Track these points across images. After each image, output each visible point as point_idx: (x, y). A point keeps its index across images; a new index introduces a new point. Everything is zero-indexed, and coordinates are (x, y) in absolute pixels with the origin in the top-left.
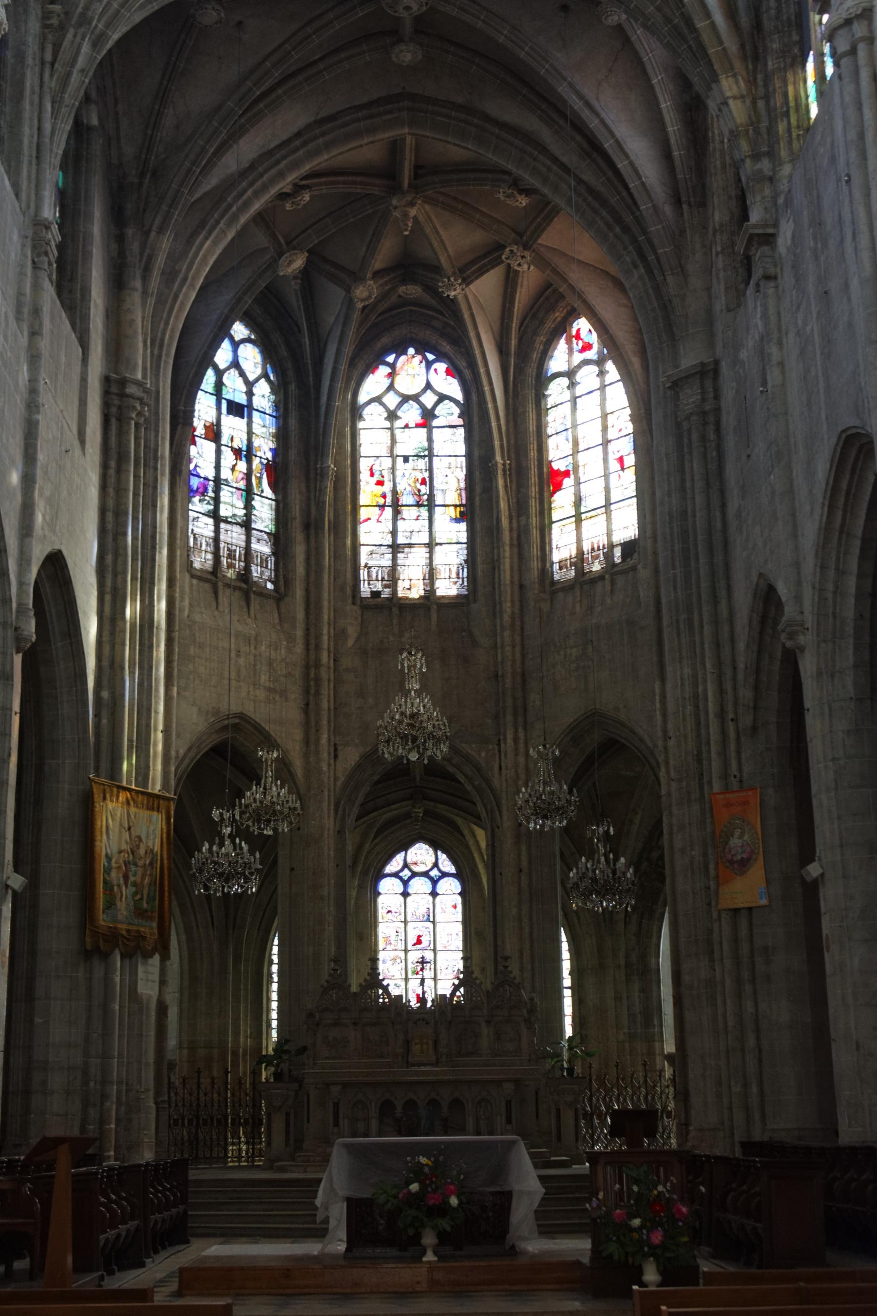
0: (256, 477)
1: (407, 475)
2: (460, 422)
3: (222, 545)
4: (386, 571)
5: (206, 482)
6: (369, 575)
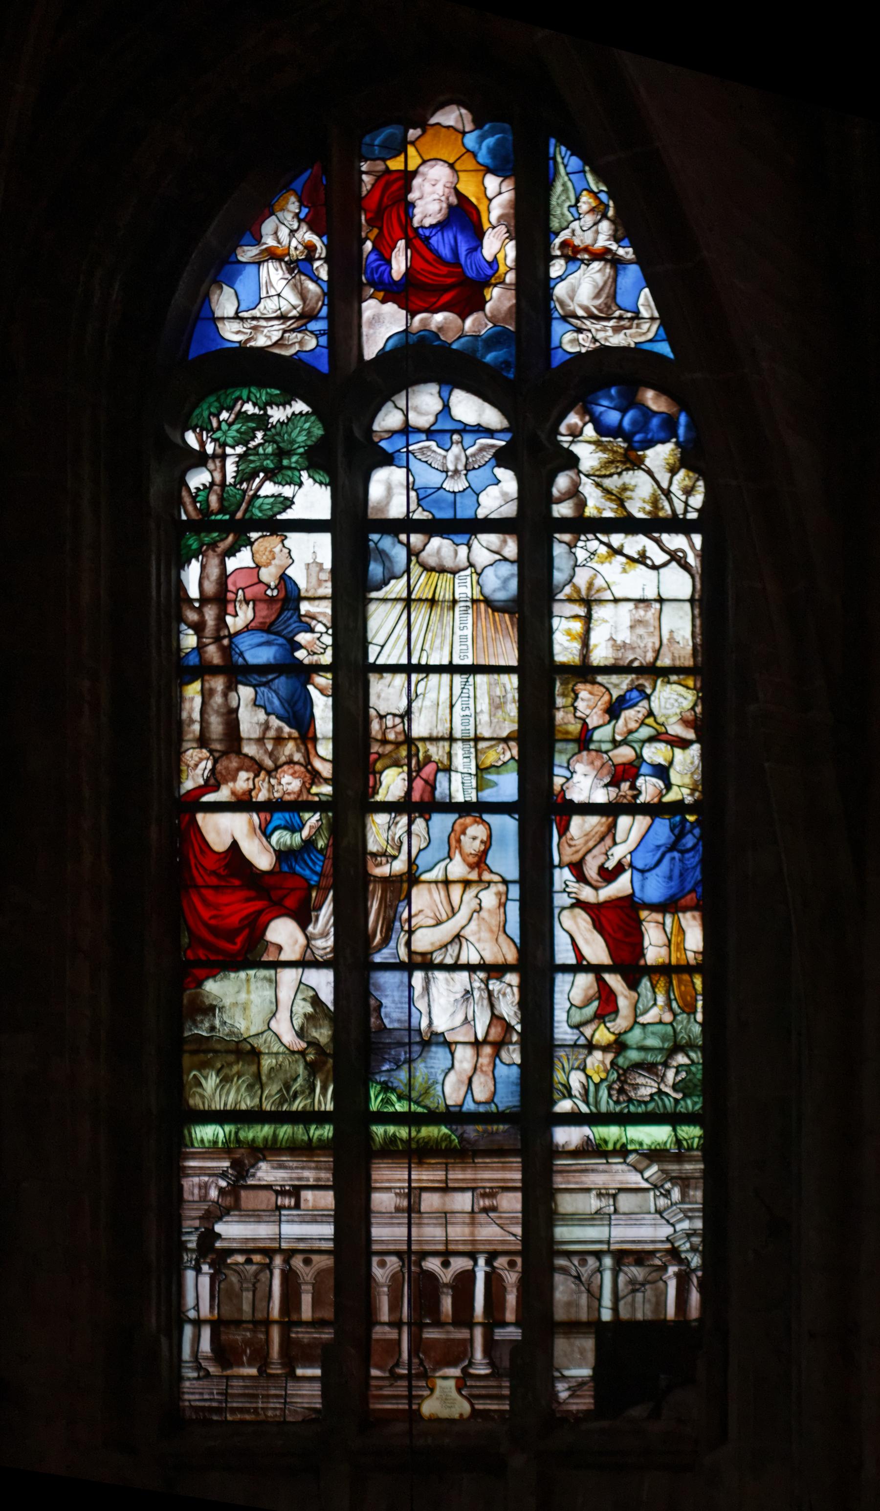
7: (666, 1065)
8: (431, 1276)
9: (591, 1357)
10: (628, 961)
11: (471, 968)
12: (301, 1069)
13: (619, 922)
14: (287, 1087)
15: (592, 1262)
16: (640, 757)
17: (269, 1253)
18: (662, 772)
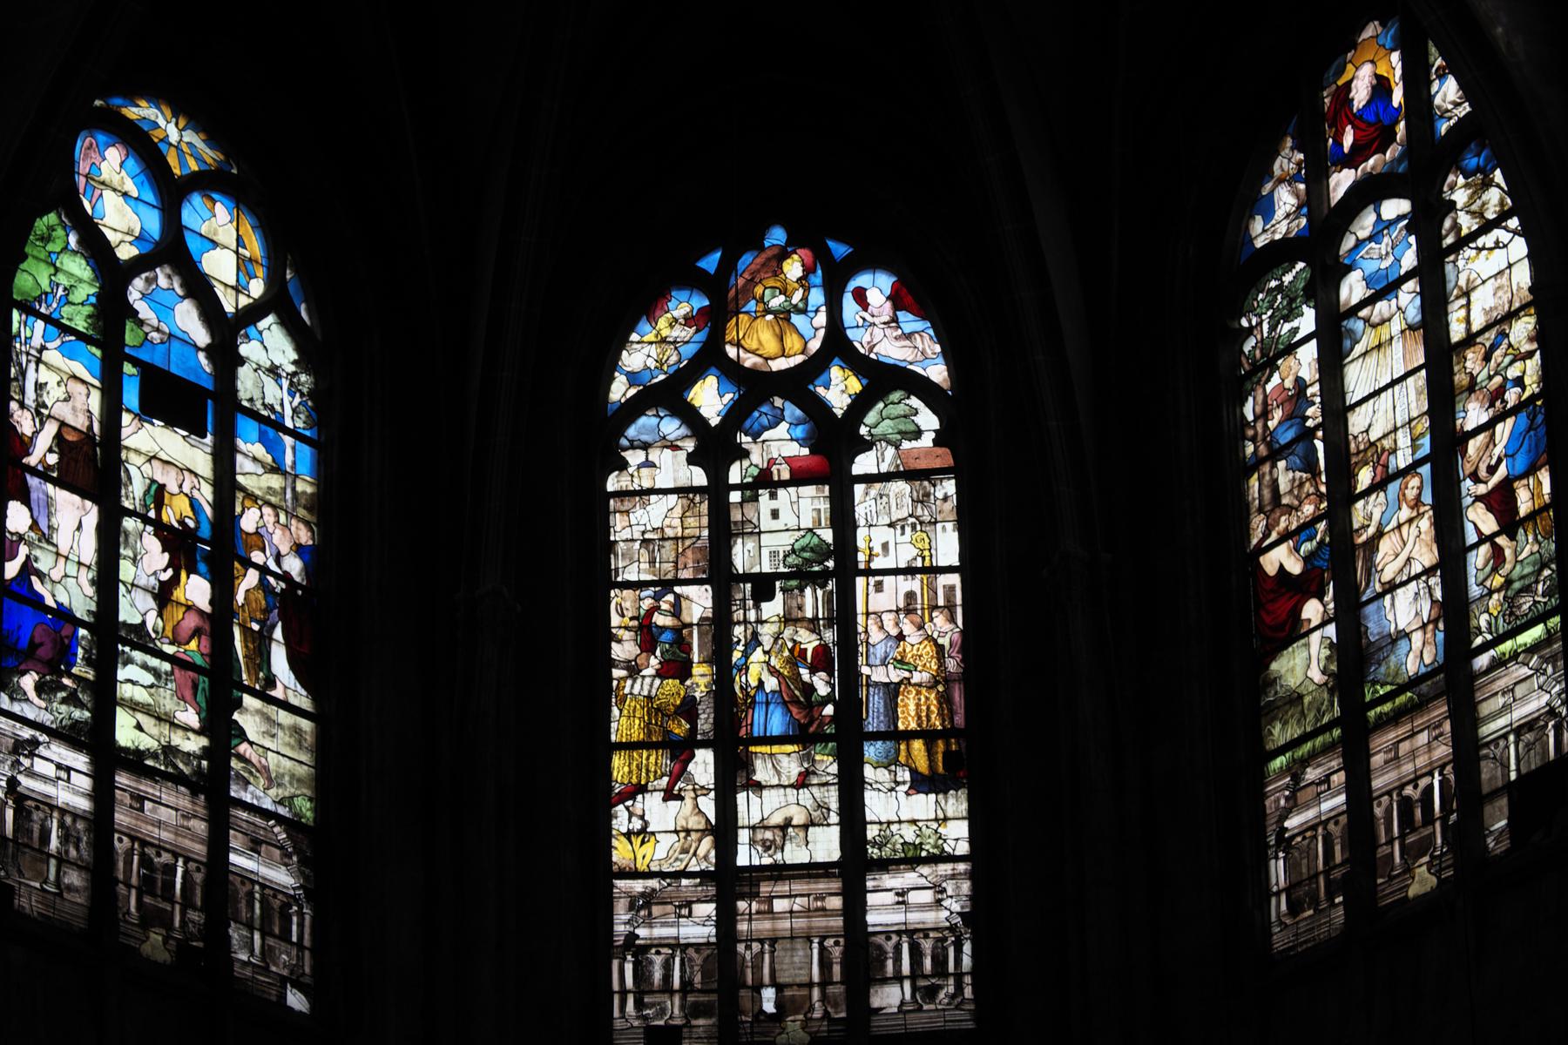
0: (246, 631)
1: (767, 641)
2: (944, 458)
3: (121, 845)
4: (698, 959)
6: (641, 973)
7: (1537, 582)
8: (1408, 798)
9: (1506, 810)
10: (1510, 523)
11: (1417, 577)
12: (1326, 695)
13: (1501, 500)
14: (1319, 710)
15: (1502, 743)
16: (1505, 379)
17: (1314, 828)
18: (1519, 382)
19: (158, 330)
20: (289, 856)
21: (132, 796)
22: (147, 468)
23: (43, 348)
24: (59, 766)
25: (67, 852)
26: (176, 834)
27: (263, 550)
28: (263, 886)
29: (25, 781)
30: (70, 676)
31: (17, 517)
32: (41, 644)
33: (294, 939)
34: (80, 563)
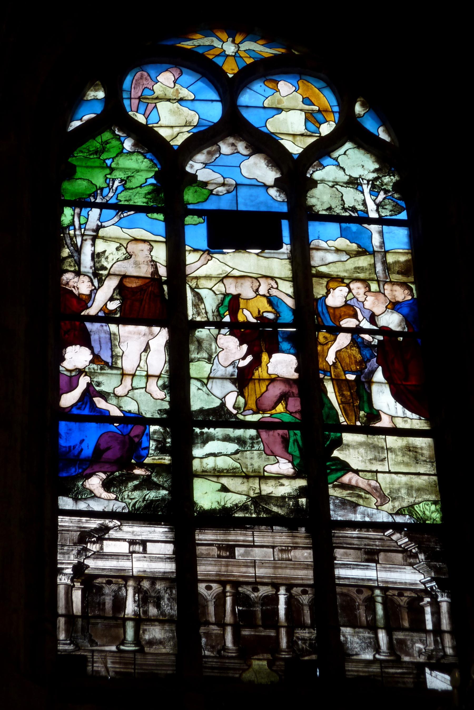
0: (340, 384)
5: (137, 430)
19: (223, 185)
20: (415, 556)
21: (220, 548)
22: (220, 288)
23: (99, 228)
24: (132, 542)
25: (146, 612)
26: (275, 568)
27: (355, 316)
28: (384, 590)
29: (91, 563)
30: (141, 465)
31: (76, 357)
32: (108, 449)
33: (429, 626)
34: (148, 376)
